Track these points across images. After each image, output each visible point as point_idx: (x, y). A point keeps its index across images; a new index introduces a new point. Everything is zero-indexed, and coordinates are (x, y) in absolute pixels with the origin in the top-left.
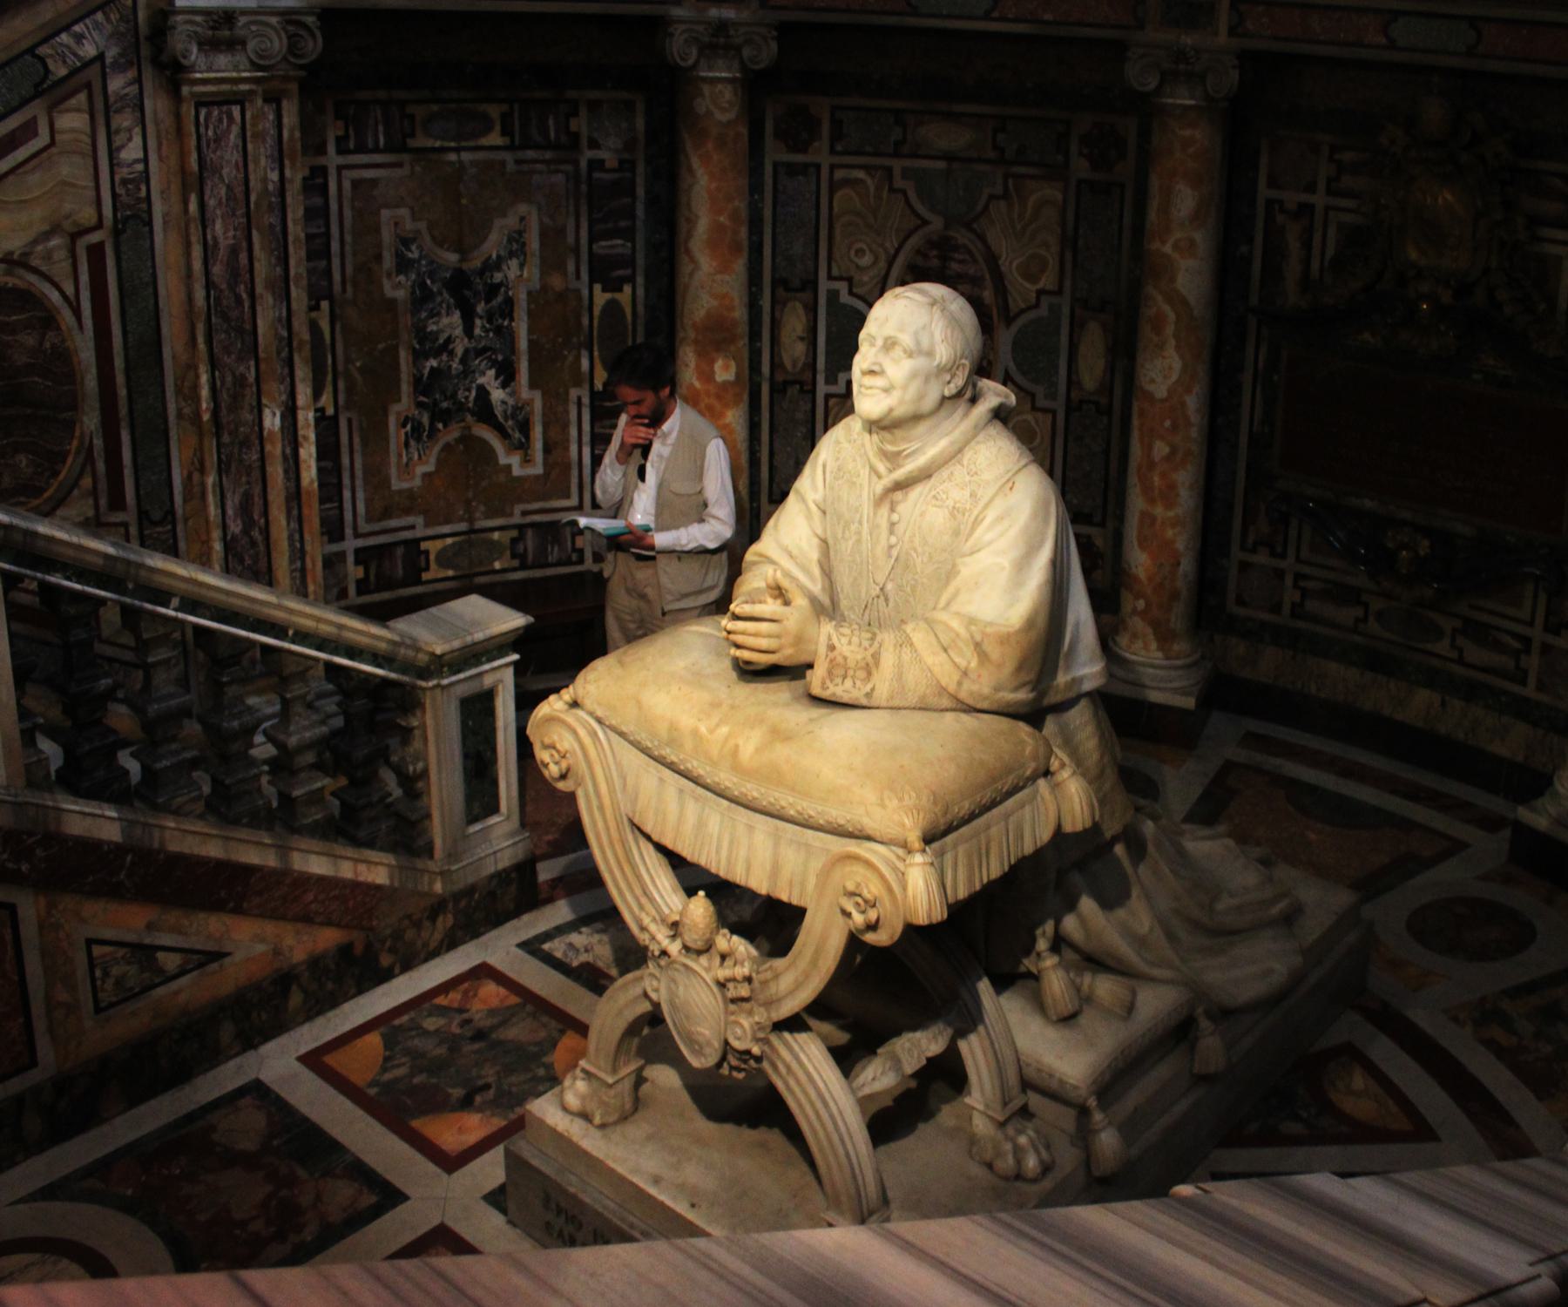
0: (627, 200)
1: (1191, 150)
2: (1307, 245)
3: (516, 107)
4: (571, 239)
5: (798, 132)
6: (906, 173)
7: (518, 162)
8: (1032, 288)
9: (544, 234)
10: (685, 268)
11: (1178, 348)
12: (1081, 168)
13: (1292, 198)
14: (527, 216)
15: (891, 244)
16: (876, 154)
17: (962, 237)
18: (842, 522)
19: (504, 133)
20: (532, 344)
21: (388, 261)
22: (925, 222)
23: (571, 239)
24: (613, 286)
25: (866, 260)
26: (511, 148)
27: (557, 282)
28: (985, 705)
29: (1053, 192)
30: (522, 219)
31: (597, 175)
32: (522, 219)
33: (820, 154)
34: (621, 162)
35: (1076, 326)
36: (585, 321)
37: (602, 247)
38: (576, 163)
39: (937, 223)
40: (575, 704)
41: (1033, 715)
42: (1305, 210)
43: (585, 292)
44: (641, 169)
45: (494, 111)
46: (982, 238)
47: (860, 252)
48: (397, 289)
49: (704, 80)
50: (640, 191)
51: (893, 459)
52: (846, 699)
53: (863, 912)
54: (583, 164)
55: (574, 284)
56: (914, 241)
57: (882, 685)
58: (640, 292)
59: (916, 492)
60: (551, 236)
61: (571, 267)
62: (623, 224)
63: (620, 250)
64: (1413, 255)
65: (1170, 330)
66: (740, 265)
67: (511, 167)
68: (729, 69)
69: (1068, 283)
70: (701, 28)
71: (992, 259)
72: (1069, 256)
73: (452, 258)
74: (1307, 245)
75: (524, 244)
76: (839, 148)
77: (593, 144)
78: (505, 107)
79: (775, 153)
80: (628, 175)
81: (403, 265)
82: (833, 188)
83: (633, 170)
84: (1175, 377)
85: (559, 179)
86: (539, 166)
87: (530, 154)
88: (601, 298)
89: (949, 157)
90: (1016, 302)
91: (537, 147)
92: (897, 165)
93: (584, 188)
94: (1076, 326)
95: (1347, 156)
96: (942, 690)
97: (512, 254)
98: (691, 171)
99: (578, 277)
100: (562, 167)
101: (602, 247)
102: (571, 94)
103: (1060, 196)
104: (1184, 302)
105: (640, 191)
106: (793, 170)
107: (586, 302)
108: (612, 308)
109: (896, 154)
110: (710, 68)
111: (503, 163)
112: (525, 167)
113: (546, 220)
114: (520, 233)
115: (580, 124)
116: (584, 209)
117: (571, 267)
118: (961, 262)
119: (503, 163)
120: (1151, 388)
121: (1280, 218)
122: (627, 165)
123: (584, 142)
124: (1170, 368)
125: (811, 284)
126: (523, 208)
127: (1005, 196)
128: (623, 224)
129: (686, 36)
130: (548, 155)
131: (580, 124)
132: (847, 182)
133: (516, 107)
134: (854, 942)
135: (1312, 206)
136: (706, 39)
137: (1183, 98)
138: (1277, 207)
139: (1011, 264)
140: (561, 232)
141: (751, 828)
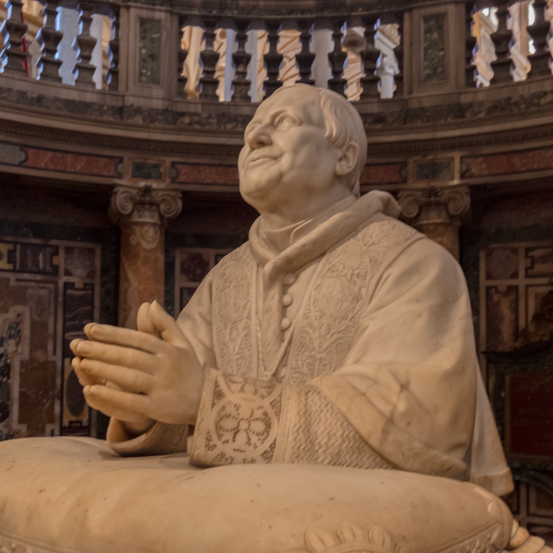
0: (88, 308)
2: (515, 310)
3: (18, 247)
4: (51, 330)
7: (18, 280)
9: (33, 325)
13: (503, 284)
23: (51, 330)
26: (14, 271)
27: (40, 356)
30: (19, 315)
31: (69, 292)
32: (19, 315)
34: (85, 285)
36: (58, 381)
38: (56, 283)
43: (59, 363)
49: (136, 223)
50: (97, 303)
54: (61, 285)
55: (51, 358)
61: (50, 347)
67: (13, 283)
68: (152, 217)
70: (135, 192)
74: (515, 310)
75: (19, 331)
77: (68, 273)
78: (11, 247)
80: (89, 292)
83: (93, 290)
85: (44, 292)
86: (32, 284)
87: (26, 276)
91: (31, 272)
93: (61, 299)
97: (11, 337)
98: (127, 279)
99: (55, 353)
100: (47, 285)
102: (54, 242)
105: (97, 303)
107: (59, 370)
110: (140, 216)
111: (8, 280)
112: (22, 284)
113: (35, 317)
114: (17, 324)
115: (60, 260)
116: (60, 312)
117: (50, 347)
119: (8, 280)
121: (496, 298)
123: (62, 271)
126: (20, 308)
129: (125, 195)
130: (38, 277)
131: (60, 260)
133: (18, 247)
135: (516, 288)
136: (138, 198)
140: (44, 325)
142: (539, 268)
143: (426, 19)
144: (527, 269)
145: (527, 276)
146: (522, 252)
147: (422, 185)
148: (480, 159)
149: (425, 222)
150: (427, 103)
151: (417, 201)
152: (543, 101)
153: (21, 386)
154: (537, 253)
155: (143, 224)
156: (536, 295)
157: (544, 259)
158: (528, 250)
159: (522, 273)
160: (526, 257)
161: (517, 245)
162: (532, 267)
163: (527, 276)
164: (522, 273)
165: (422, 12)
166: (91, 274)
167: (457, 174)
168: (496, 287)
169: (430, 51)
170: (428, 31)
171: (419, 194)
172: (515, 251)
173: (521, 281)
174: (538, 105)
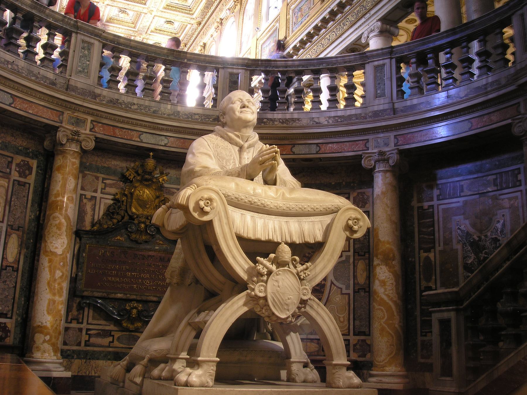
1: (75, 166)
2: (94, 210)
11: (66, 235)
12: (15, 175)
13: (89, 194)
18: (224, 161)
35: (8, 235)
42: (94, 198)
64: (134, 210)
65: (64, 229)
69: (6, 218)
72: (7, 208)
74: (94, 210)
84: (65, 246)
103: (7, 185)
104: (69, 218)
120: (56, 250)
121: (85, 201)
124: (64, 243)
135: (96, 197)
137: (74, 148)
138: (84, 196)
142: (108, 190)
143: (83, 41)
144: (102, 189)
145: (102, 193)
146: (101, 179)
147: (70, 127)
148: (100, 125)
149: (69, 149)
150: (79, 85)
151: (67, 136)
152: (132, 107)
154: (108, 182)
156: (105, 204)
157: (111, 186)
158: (104, 179)
159: (99, 191)
160: (103, 182)
161: (99, 175)
162: (105, 189)
163: (102, 193)
164: (99, 191)
165: (83, 37)
167: (88, 129)
168: (85, 195)
169: (83, 59)
170: (83, 48)
171: (69, 132)
172: (97, 178)
173: (98, 195)
174: (131, 108)
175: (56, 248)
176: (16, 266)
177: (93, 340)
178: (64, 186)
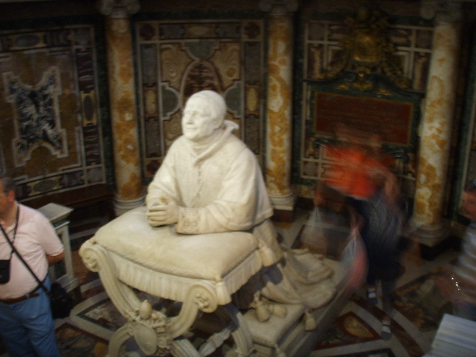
5: (147, 33)
6: (187, 44)
8: (231, 79)
10: (112, 83)
12: (245, 38)
13: (316, 42)
14: (55, 70)
15: (182, 68)
16: (176, 39)
17: (206, 64)
19: (45, 42)
20: (62, 114)
21: (7, 90)
22: (193, 60)
24: (87, 91)
25: (174, 75)
27: (67, 92)
28: (236, 229)
29: (236, 47)
31: (79, 54)
32: (54, 71)
33: (156, 41)
35: (246, 90)
37: (83, 78)
39: (197, 60)
40: (95, 243)
41: (250, 230)
42: (321, 46)
44: (94, 51)
45: (40, 35)
46: (213, 64)
47: (172, 72)
48: (11, 99)
51: (198, 151)
52: (189, 232)
53: (203, 303)
56: (190, 67)
57: (201, 227)
58: (97, 92)
59: (206, 162)
60: (64, 76)
62: (89, 70)
63: (89, 79)
64: (357, 59)
66: (131, 81)
71: (217, 71)
73: (29, 87)
74: (321, 57)
76: (163, 37)
77: (77, 44)
79: (140, 41)
81: (12, 91)
82: (162, 51)
86: (57, 53)
87: (55, 49)
88: (84, 95)
89: (200, 38)
90: (226, 84)
92: (183, 42)
94: (246, 90)
95: (334, 28)
96: (221, 226)
97: (51, 84)
101: (83, 78)
102: (68, 27)
105: (94, 58)
106: (148, 46)
108: (88, 99)
109: (182, 38)
115: (71, 37)
118: (206, 72)
122: (89, 50)
125: (155, 84)
126: (54, 68)
127: (220, 49)
128: (89, 70)
131: (71, 37)
132: (166, 49)
134: (200, 311)
139: (223, 71)
141: (160, 278)
142: (335, 36)
153: (60, 108)
155: (118, 19)
157: (337, 32)
159: (326, 37)
166: (89, 43)
173: (325, 42)
175: (273, 107)
176: (256, 114)
177: (328, 173)
178: (275, 50)
